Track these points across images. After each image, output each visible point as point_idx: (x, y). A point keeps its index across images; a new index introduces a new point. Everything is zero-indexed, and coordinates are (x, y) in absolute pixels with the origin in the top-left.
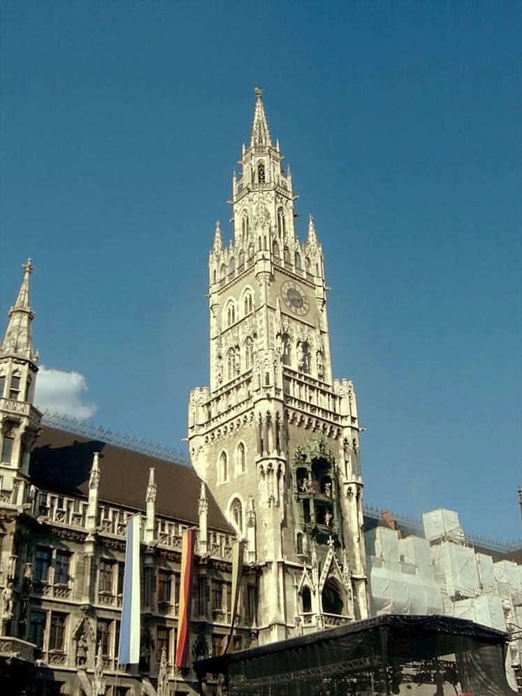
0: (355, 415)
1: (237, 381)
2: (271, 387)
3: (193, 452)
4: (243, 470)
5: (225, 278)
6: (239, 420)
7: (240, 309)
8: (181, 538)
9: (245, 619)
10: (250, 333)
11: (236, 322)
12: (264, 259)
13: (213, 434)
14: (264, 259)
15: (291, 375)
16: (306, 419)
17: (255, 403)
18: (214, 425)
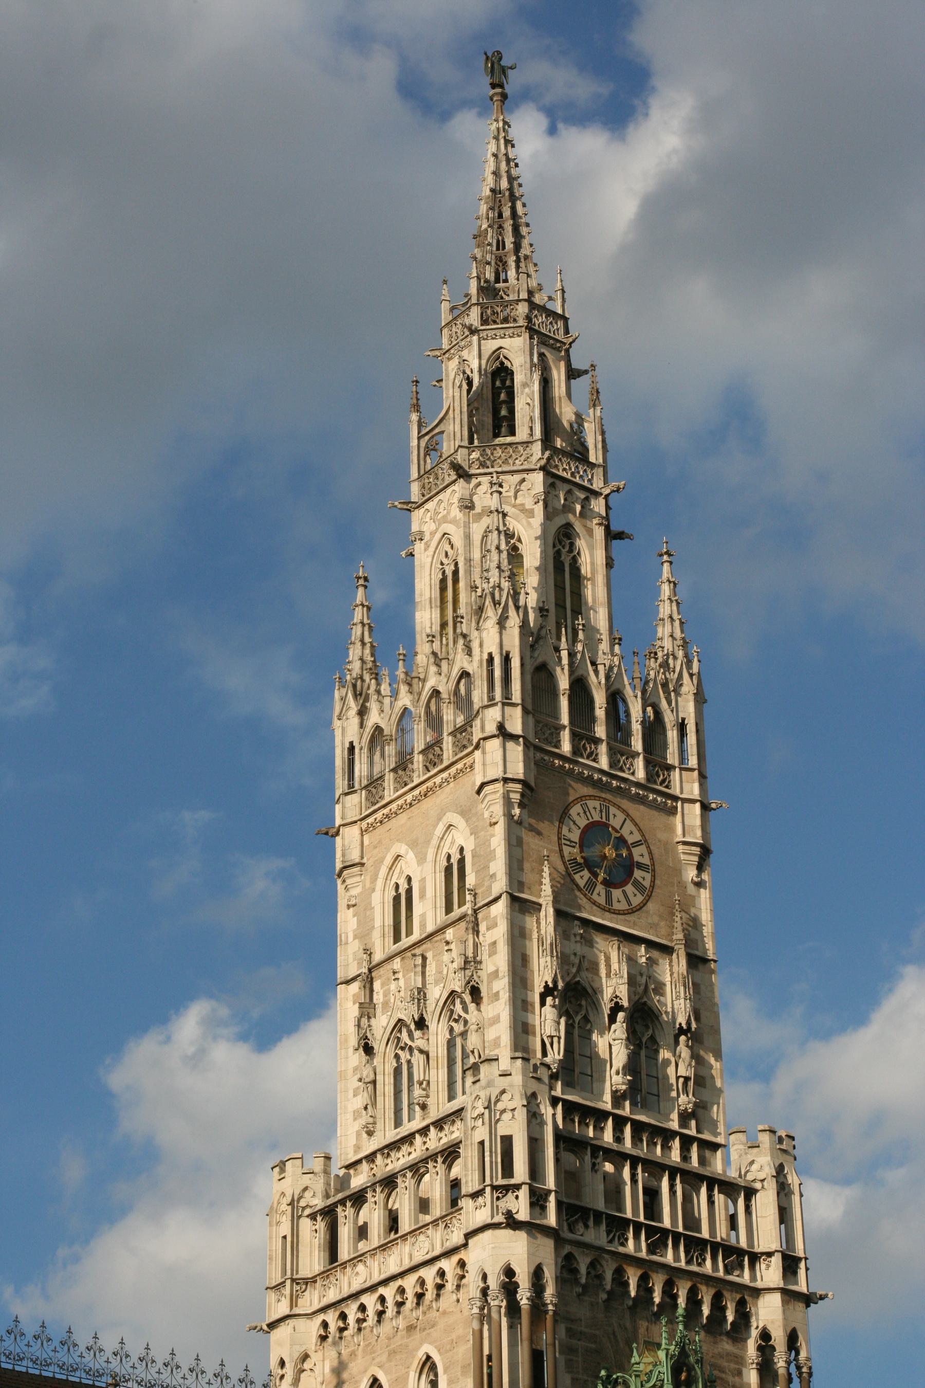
1: (418, 1139)
2: (517, 1187)
3: (280, 1372)
6: (422, 1282)
7: (430, 893)
11: (416, 936)
12: (503, 732)
13: (343, 1317)
14: (503, 732)
17: (469, 1236)
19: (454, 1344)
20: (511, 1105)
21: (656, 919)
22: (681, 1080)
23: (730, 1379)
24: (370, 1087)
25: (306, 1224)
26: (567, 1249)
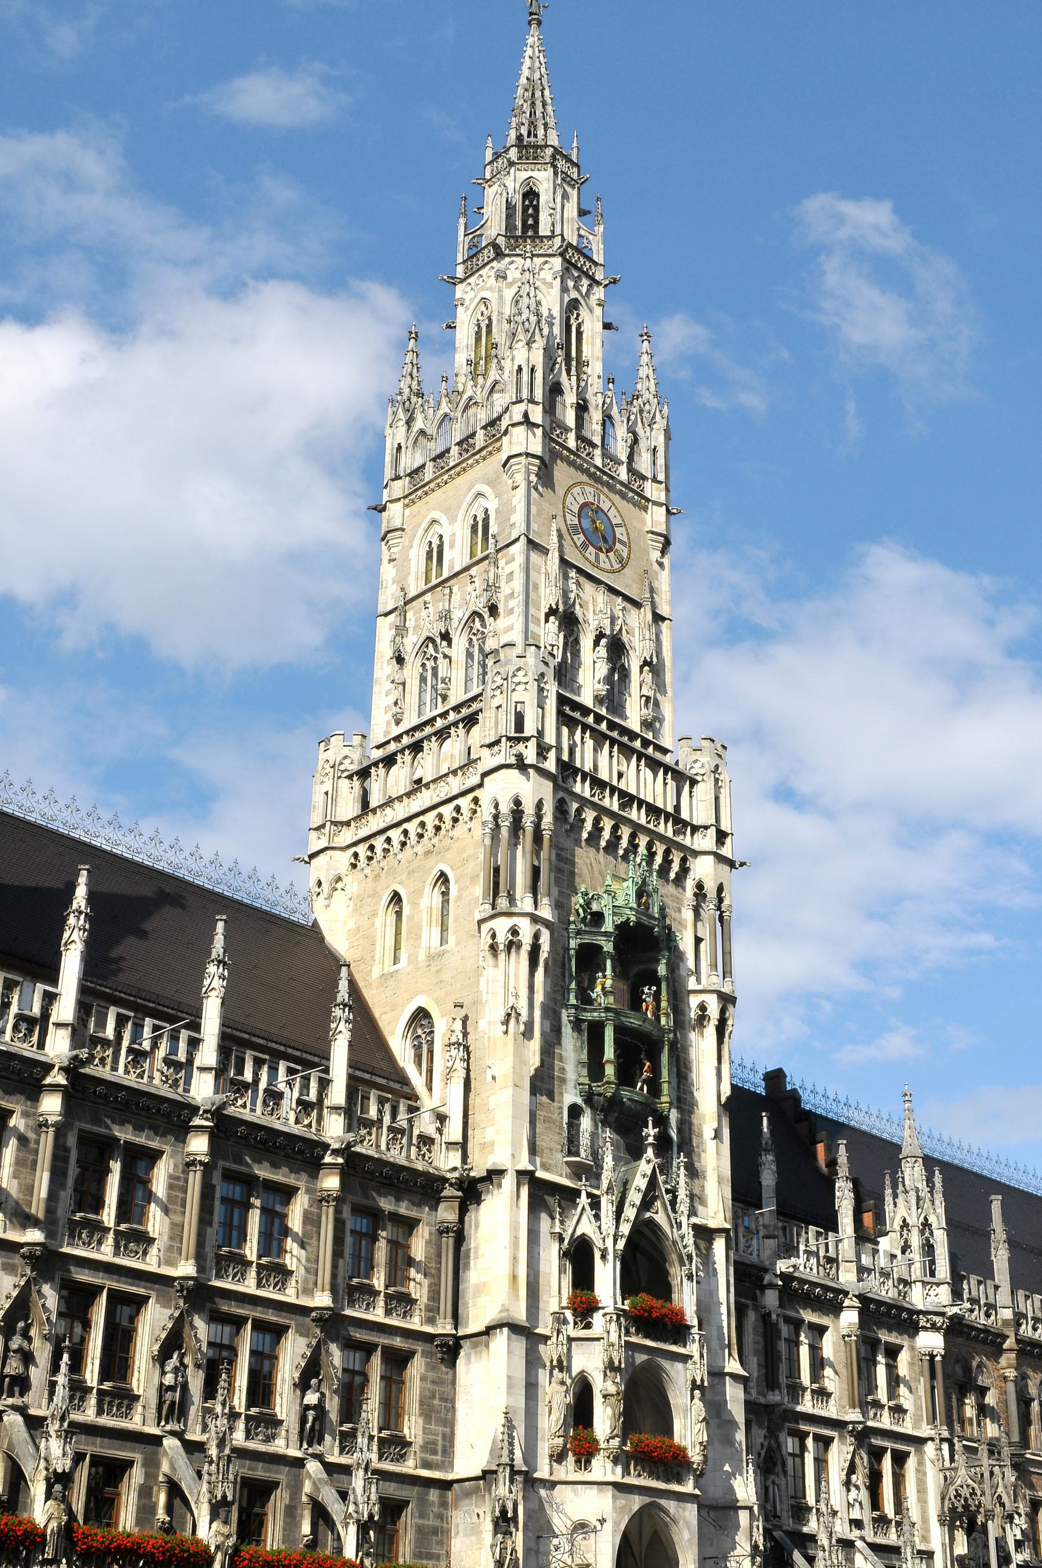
0: (725, 826)
2: (527, 739)
4: (443, 941)
5: (423, 466)
6: (440, 817)
8: (280, 1095)
9: (428, 1309)
10: (480, 604)
12: (526, 421)
13: (372, 848)
15: (577, 715)
16: (607, 824)
18: (375, 823)
19: (465, 861)
20: (525, 680)
21: (630, 582)
22: (644, 699)
23: (673, 914)
24: (401, 687)
25: (344, 783)
26: (561, 794)
